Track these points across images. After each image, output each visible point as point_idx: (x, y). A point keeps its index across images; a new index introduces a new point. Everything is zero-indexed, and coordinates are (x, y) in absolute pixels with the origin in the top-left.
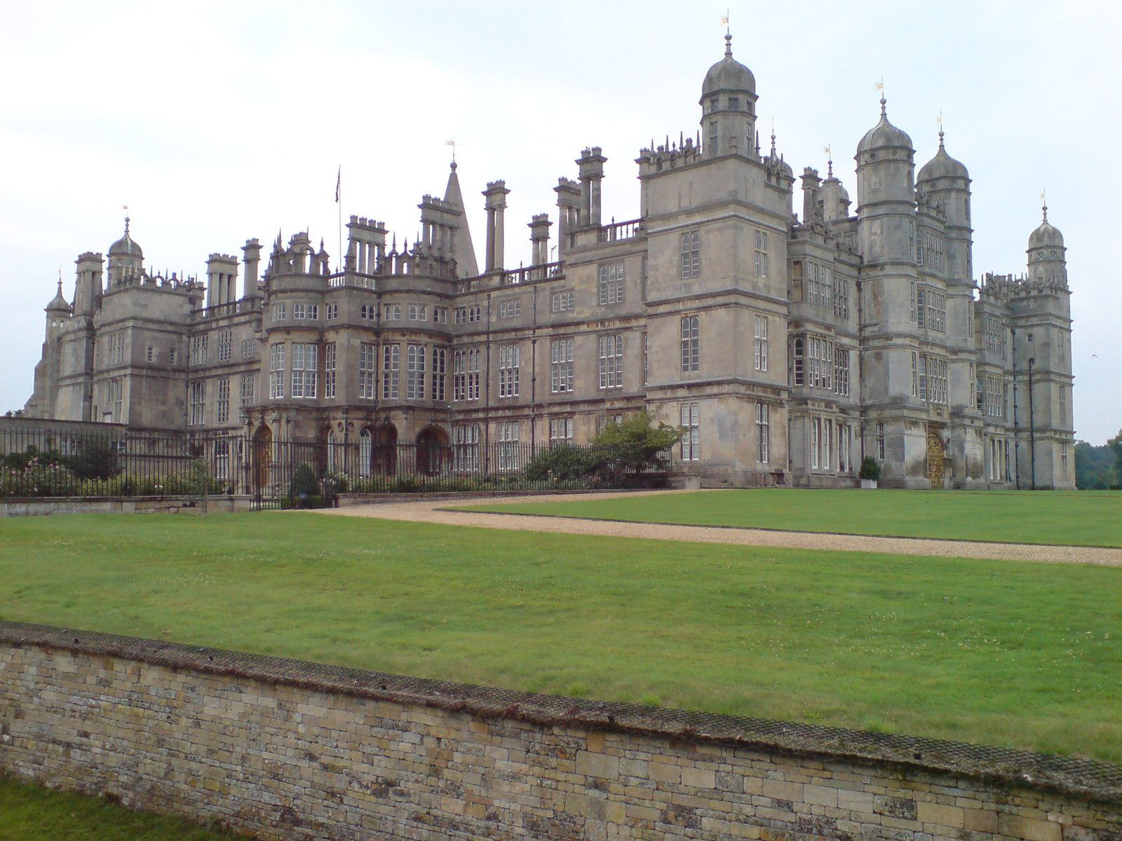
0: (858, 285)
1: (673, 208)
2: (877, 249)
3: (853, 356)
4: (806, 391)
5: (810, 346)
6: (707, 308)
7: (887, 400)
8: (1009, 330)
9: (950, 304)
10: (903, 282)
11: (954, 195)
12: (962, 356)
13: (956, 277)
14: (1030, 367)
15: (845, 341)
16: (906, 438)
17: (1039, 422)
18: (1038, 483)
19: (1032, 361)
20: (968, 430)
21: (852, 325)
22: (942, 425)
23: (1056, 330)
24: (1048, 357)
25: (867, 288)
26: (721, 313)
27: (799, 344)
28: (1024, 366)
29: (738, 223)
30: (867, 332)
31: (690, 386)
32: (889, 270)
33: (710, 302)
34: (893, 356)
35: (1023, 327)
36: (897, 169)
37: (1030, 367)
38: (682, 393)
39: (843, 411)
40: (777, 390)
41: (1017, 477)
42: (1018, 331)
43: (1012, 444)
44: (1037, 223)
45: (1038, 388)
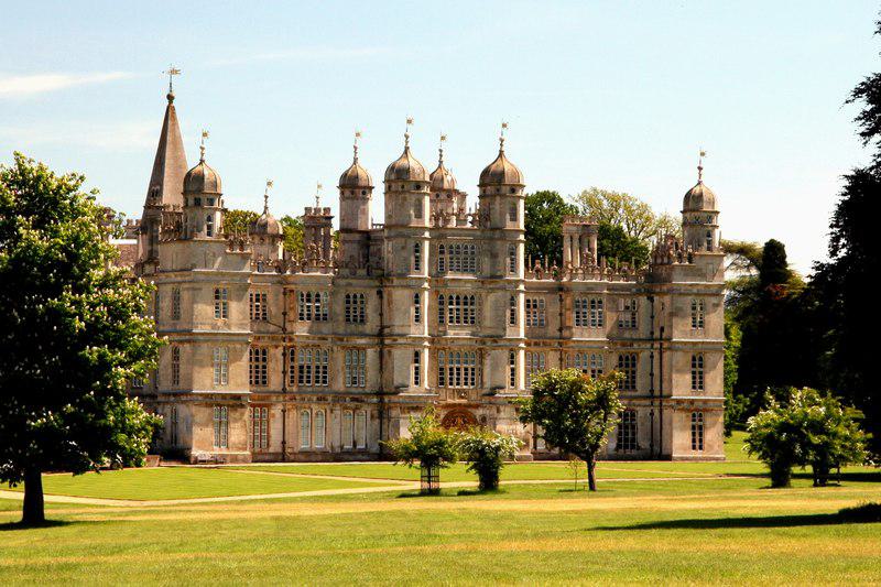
0: (380, 293)
1: (169, 268)
2: (390, 265)
3: (371, 354)
4: (295, 389)
5: (298, 355)
6: (181, 342)
7: (393, 390)
8: (643, 300)
9: (491, 298)
10: (406, 292)
11: (498, 198)
12: (502, 343)
13: (499, 274)
14: (661, 335)
15: (362, 341)
16: (401, 421)
17: (665, 393)
18: (664, 452)
19: (662, 330)
20: (502, 408)
21: (371, 325)
22: (477, 406)
23: (690, 298)
24: (671, 327)
25: (385, 296)
26: (187, 345)
27: (293, 353)
28: (657, 334)
29: (196, 285)
30: (386, 331)
31: (175, 395)
32: (396, 282)
33: (183, 338)
34: (397, 353)
35: (658, 294)
36: (405, 199)
37: (661, 335)
38: (172, 399)
39: (353, 400)
40: (237, 397)
41: (652, 446)
42: (656, 298)
43: (641, 412)
44: (689, 183)
45: (666, 355)
